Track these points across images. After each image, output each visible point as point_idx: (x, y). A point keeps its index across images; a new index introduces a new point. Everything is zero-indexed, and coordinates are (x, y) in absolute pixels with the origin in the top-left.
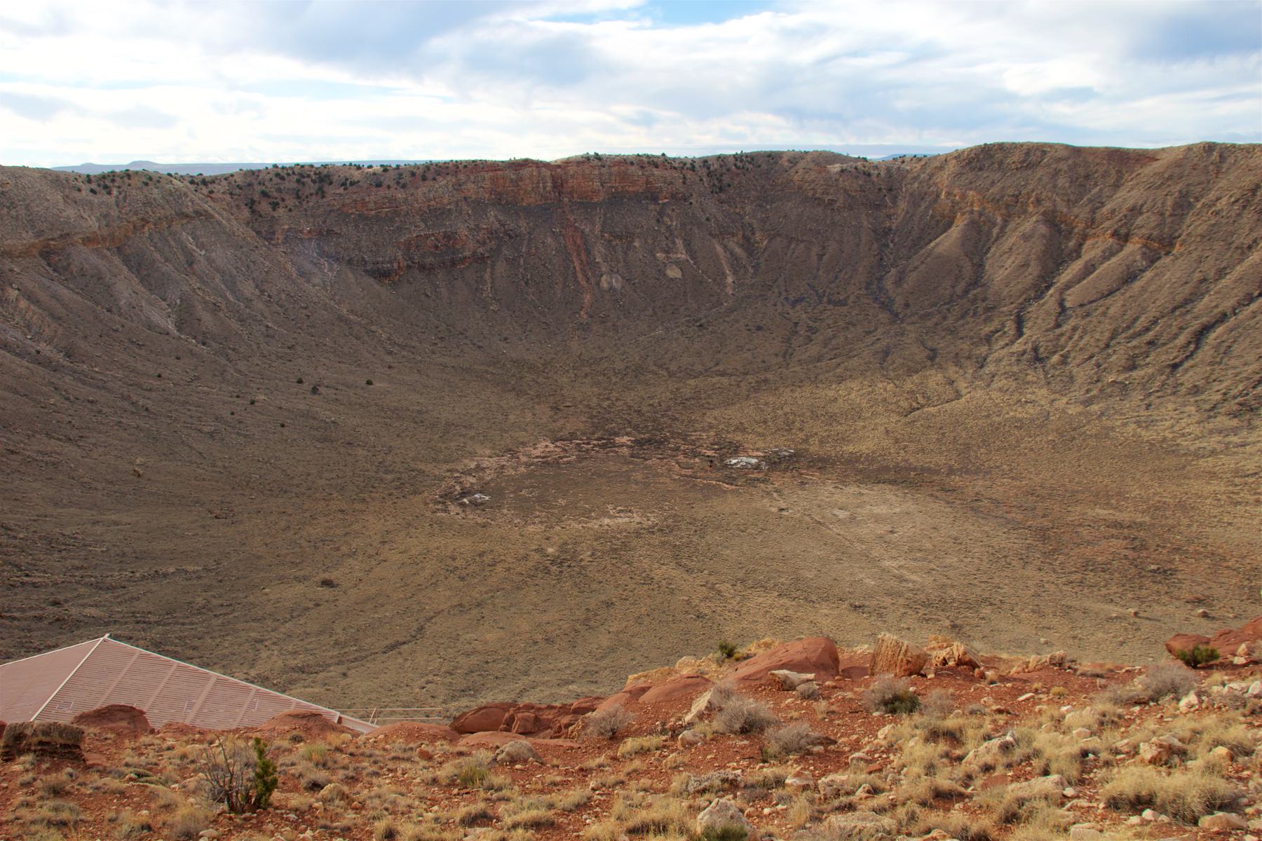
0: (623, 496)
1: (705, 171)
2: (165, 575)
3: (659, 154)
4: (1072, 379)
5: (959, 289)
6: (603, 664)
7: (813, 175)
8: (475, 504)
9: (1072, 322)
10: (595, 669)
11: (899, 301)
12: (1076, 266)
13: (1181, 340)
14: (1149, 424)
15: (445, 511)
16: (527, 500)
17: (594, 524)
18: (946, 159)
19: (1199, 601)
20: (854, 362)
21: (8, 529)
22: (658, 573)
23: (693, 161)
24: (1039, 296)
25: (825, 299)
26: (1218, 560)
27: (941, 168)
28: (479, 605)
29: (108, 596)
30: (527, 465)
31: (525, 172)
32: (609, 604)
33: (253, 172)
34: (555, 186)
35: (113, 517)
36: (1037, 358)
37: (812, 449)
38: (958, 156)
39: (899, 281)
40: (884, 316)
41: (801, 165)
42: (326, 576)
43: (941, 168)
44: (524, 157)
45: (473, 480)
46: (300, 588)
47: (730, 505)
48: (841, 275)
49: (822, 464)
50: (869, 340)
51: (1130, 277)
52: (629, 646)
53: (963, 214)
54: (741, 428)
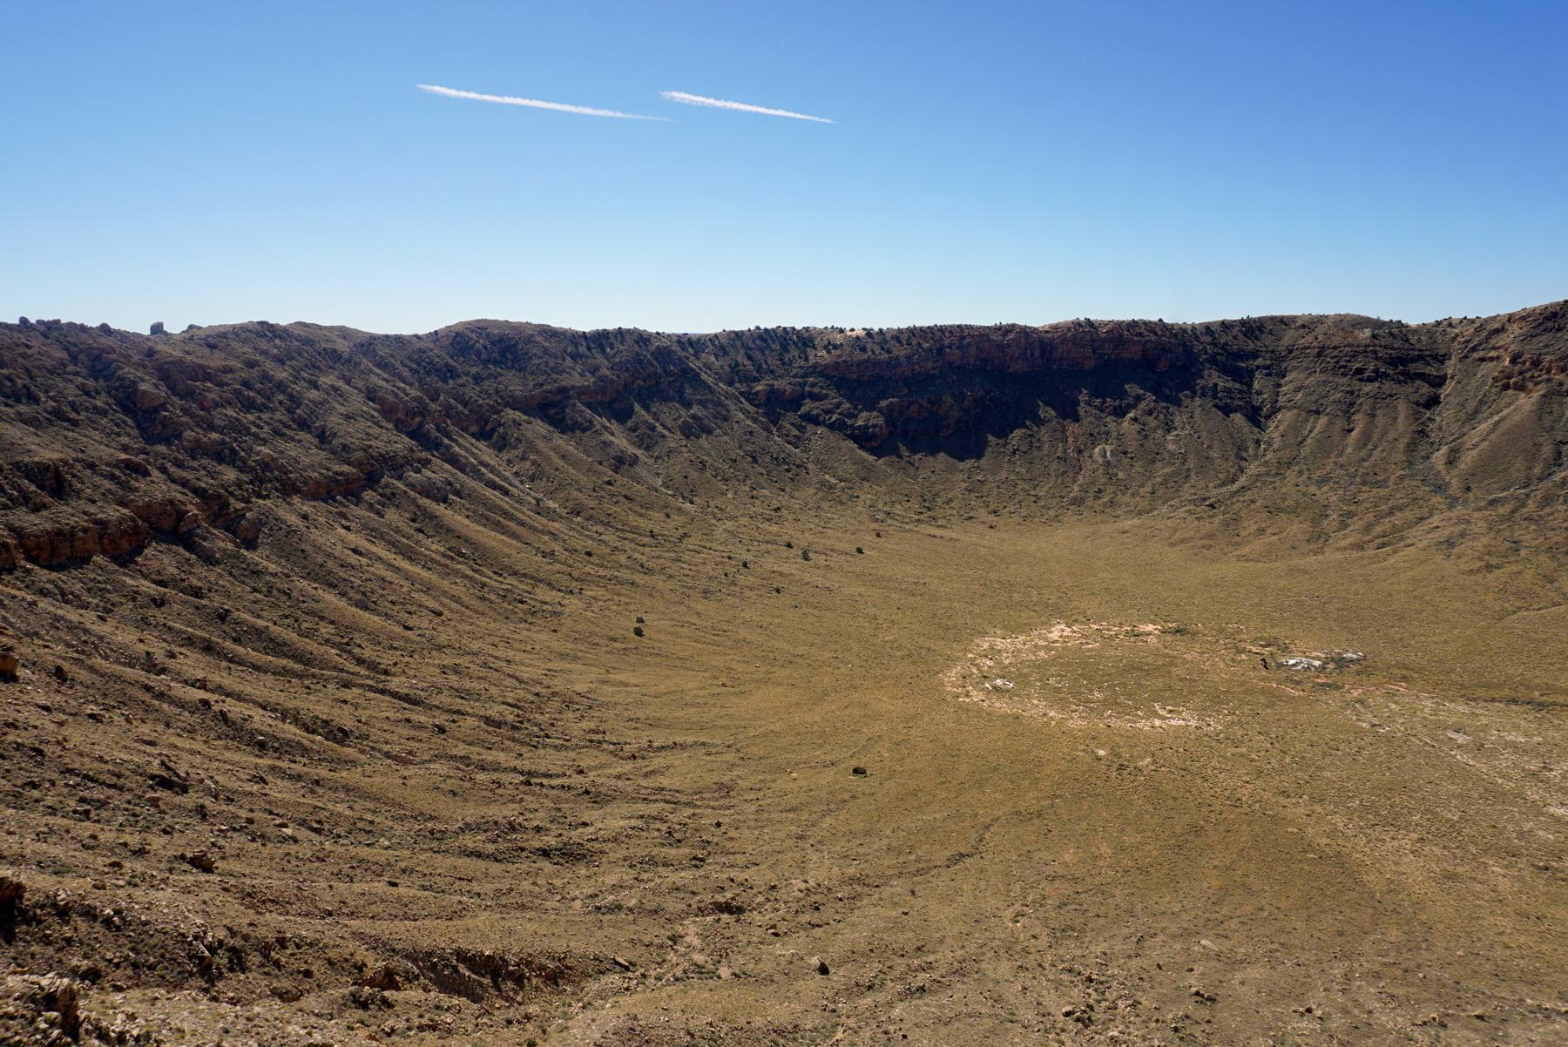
0: (1168, 694)
1: (1208, 339)
2: (683, 747)
3: (1155, 319)
5: (1537, 471)
7: (1336, 341)
8: (996, 688)
10: (1220, 918)
15: (967, 696)
16: (1058, 690)
17: (1144, 725)
18: (1510, 318)
21: (521, 682)
23: (1194, 327)
25: (1358, 479)
27: (1501, 330)
28: (1039, 815)
29: (628, 766)
30: (1047, 649)
31: (1012, 336)
32: (1197, 831)
33: (736, 333)
34: (1042, 354)
35: (620, 677)
38: (1523, 317)
41: (1320, 329)
42: (854, 763)
43: (1501, 330)
44: (1010, 322)
45: (990, 663)
46: (828, 776)
48: (1376, 453)
53: (1537, 384)
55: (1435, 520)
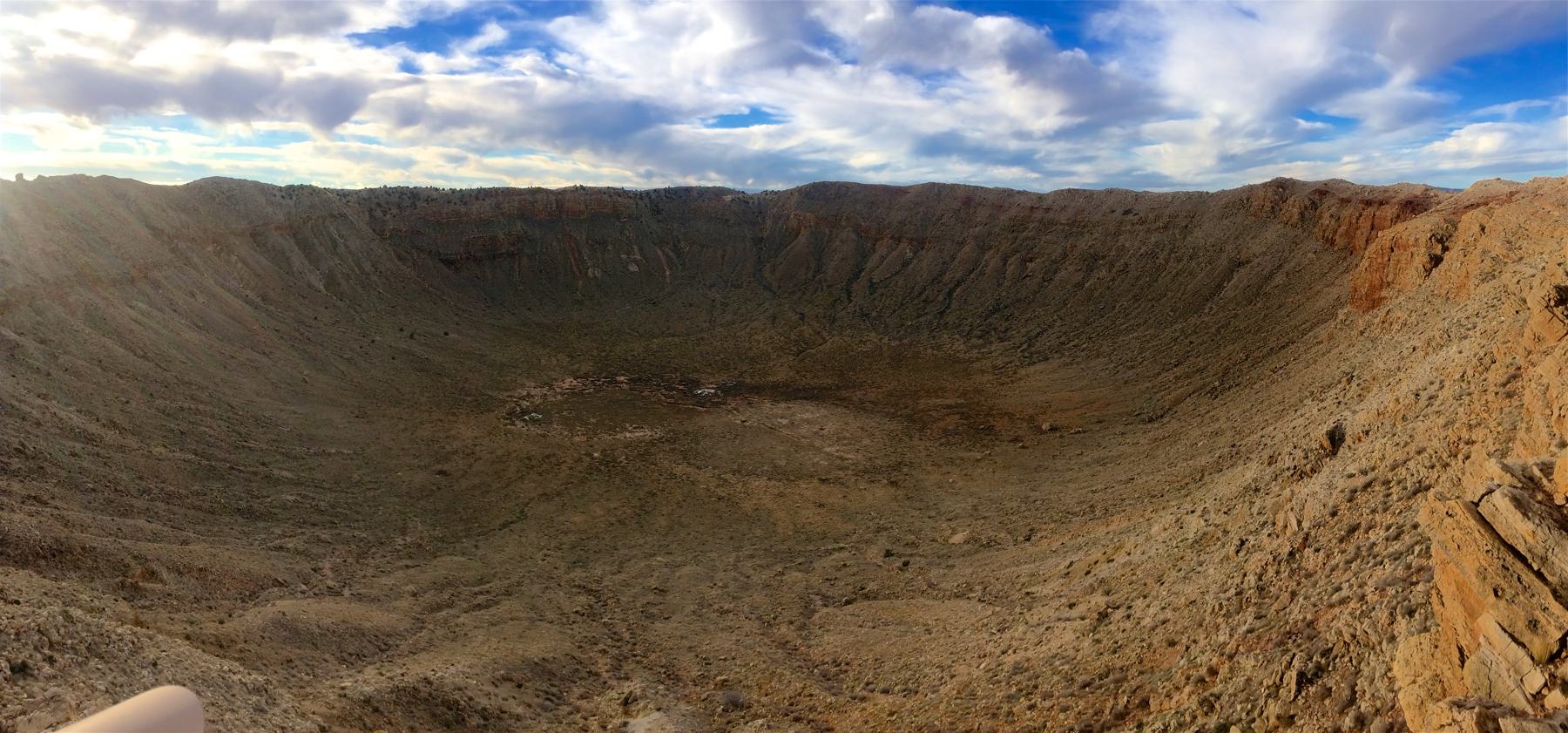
4: (886, 326)
5: (810, 275)
6: (670, 538)
9: (880, 291)
11: (775, 285)
12: (875, 258)
13: (941, 298)
14: (939, 347)
19: (1016, 440)
20: (755, 324)
22: (679, 469)
24: (857, 276)
26: (1011, 416)
36: (865, 315)
37: (748, 381)
39: (773, 272)
40: (767, 294)
47: (707, 421)
49: (757, 390)
50: (762, 309)
51: (905, 264)
52: (680, 524)
54: (696, 370)
55: (767, 305)
